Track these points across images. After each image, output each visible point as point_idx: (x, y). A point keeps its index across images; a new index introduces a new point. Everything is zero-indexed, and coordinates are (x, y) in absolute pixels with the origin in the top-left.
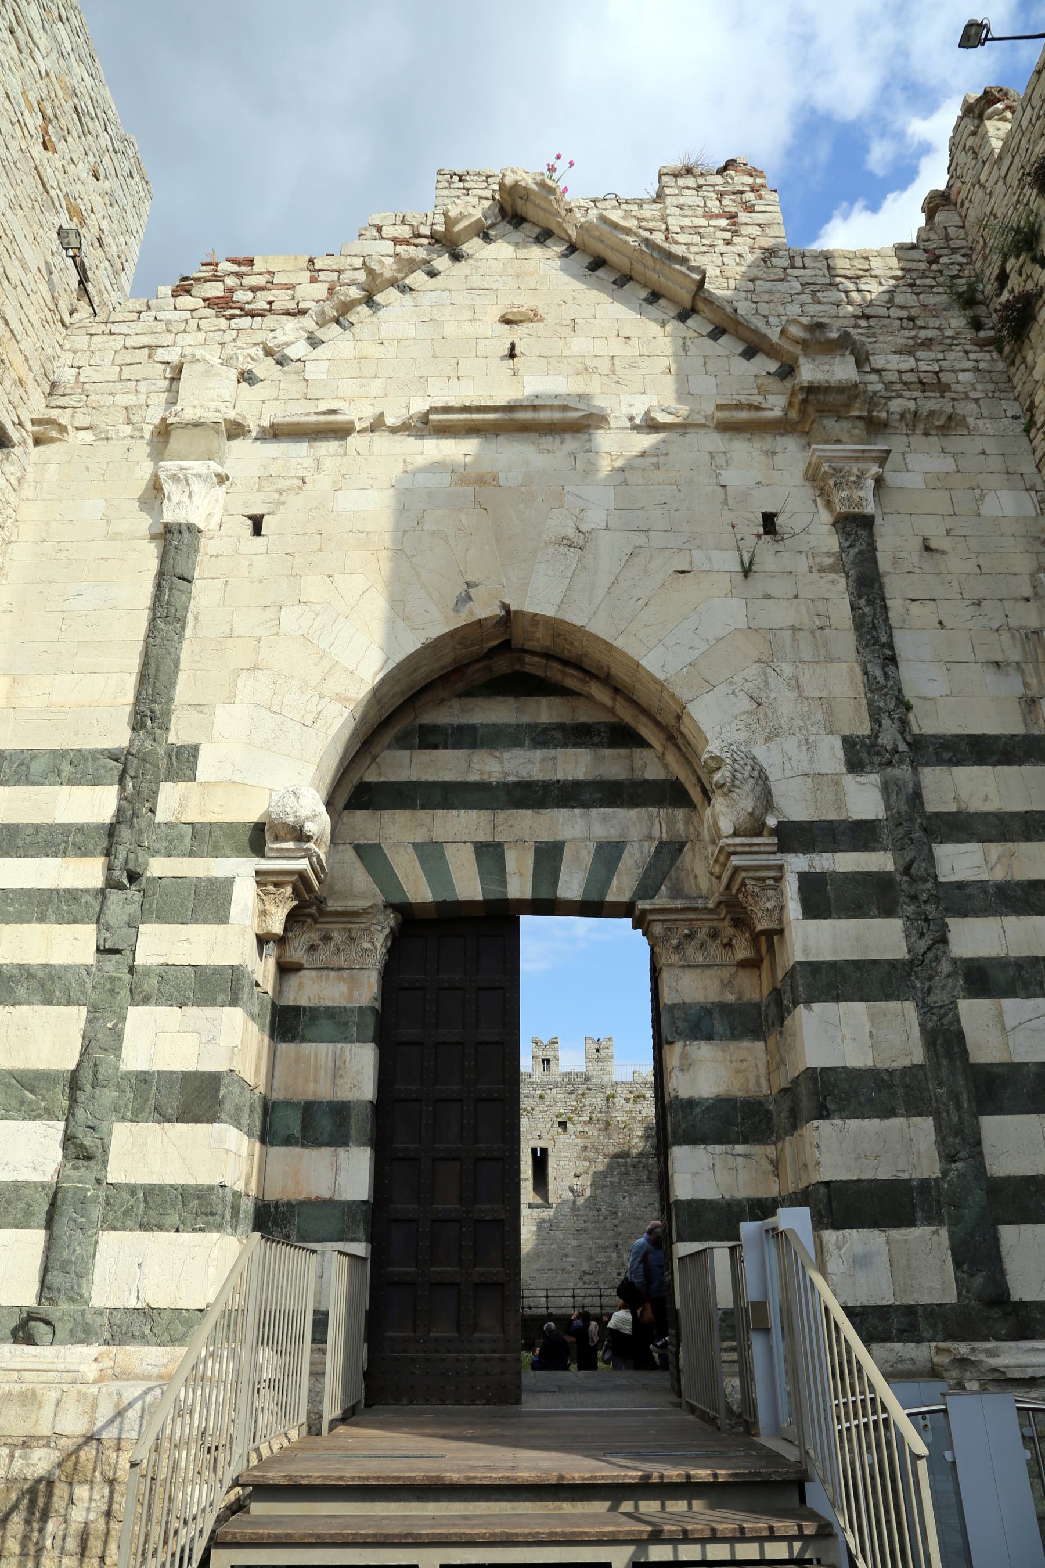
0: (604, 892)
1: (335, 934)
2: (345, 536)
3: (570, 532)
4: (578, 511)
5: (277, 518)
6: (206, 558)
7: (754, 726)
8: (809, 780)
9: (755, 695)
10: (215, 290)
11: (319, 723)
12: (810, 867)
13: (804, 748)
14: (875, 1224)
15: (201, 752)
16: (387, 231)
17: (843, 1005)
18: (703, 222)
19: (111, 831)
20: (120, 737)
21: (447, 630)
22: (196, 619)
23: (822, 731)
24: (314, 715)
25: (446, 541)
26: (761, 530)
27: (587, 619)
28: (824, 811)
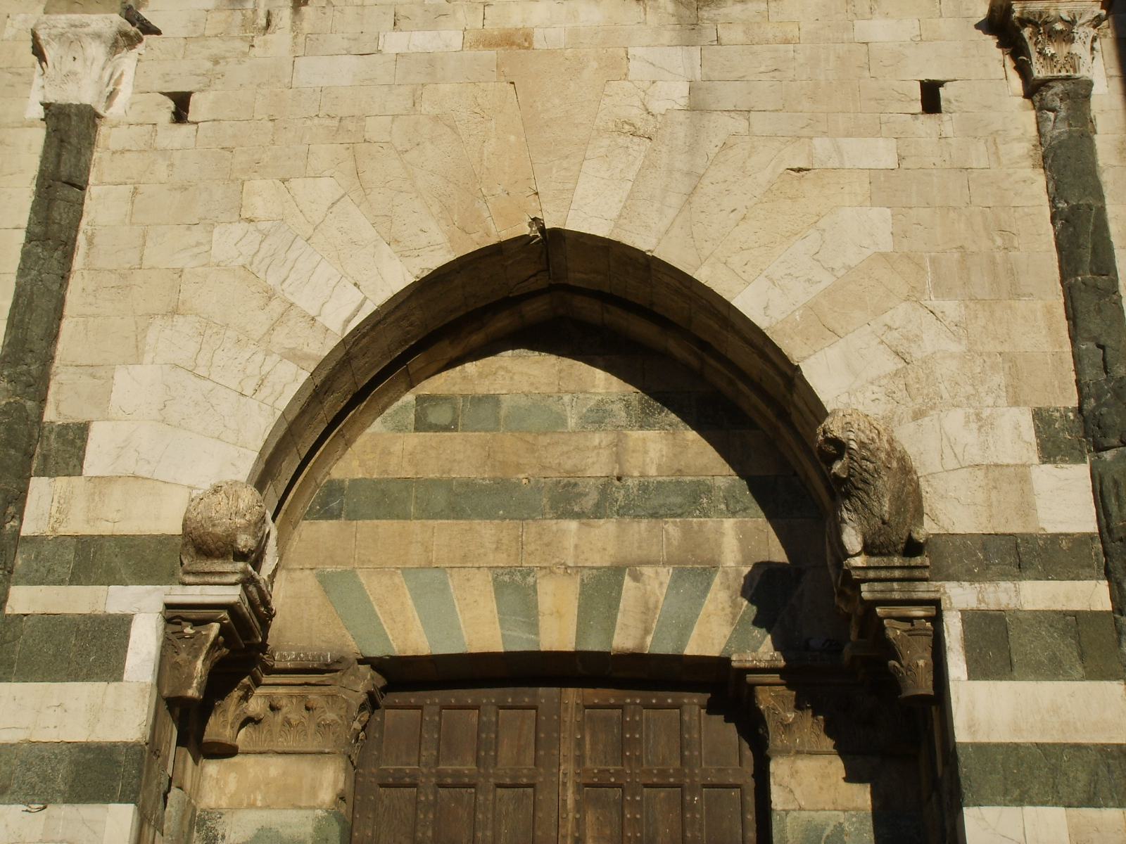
0: (683, 646)
1: (284, 702)
2: (309, 122)
3: (636, 114)
4: (647, 84)
5: (212, 95)
6: (107, 156)
7: (898, 395)
8: (980, 474)
9: (900, 349)
11: (265, 391)
12: (980, 601)
13: (974, 426)
15: (91, 434)
17: (1028, 809)
21: (451, 257)
22: (90, 242)
23: (1002, 401)
24: (256, 380)
25: (454, 129)
26: (918, 107)
27: (654, 241)
28: (1003, 521)
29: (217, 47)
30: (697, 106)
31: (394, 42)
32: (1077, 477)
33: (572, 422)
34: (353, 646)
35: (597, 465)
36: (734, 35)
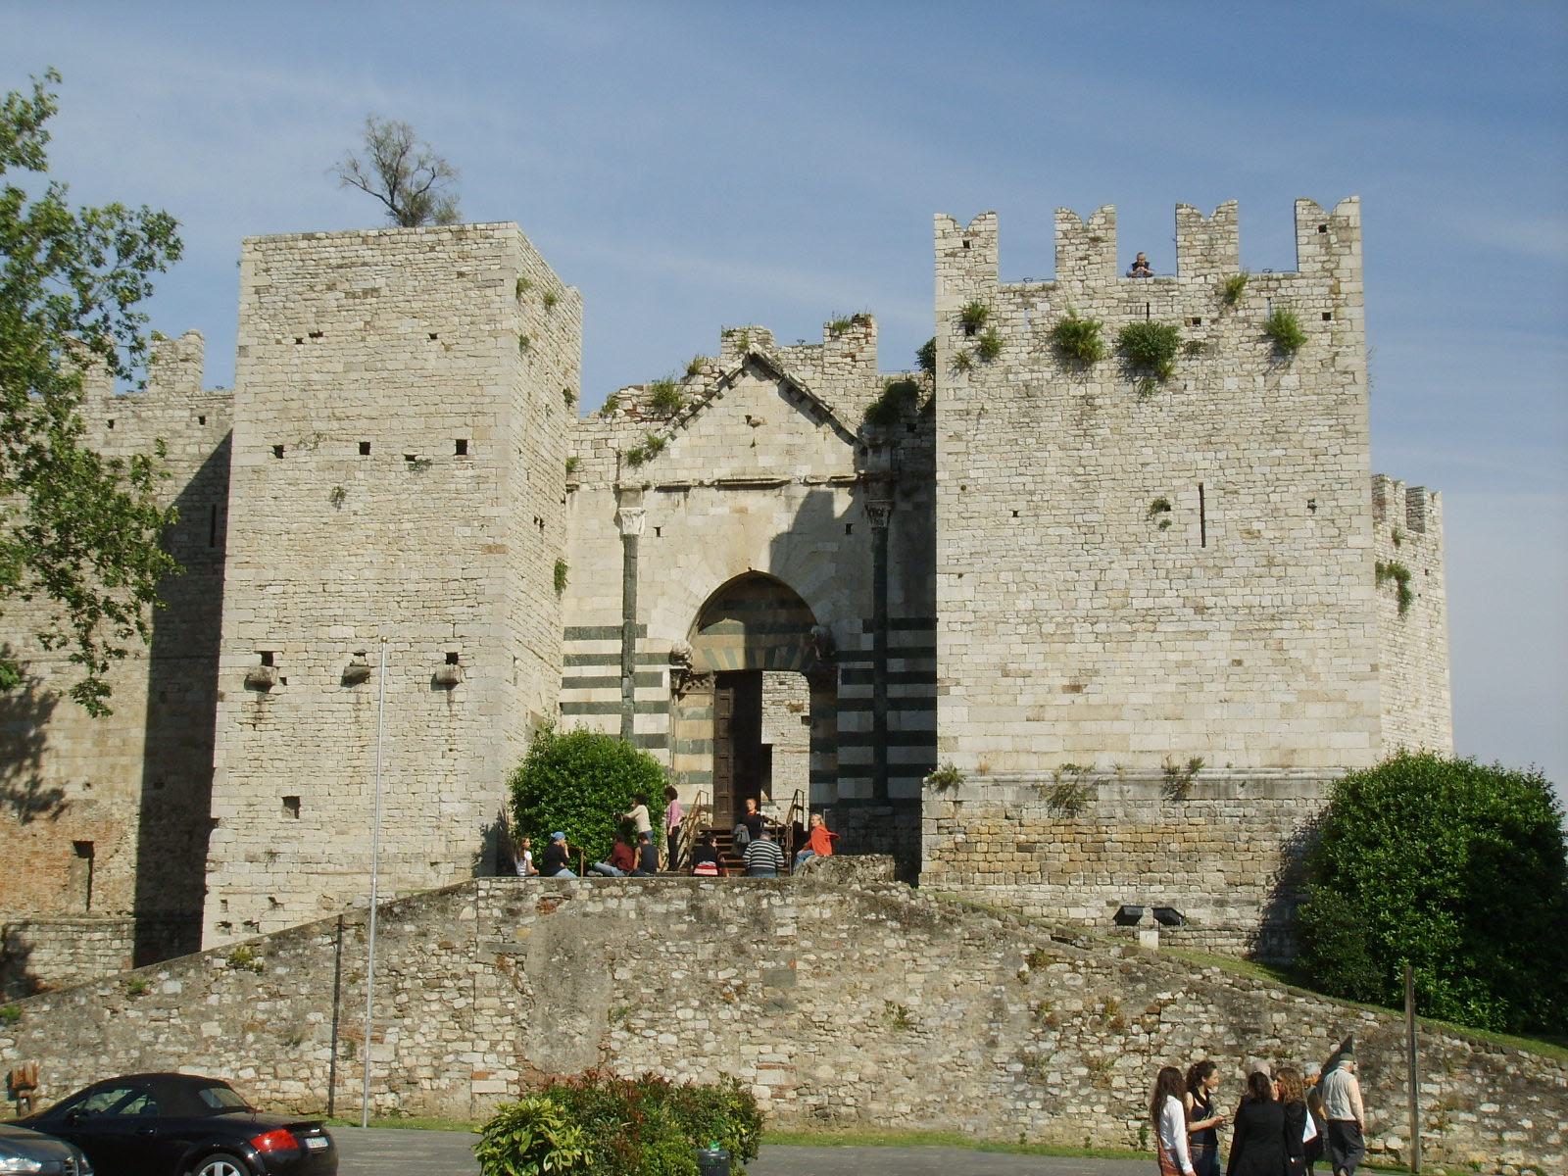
14: (850, 776)
18: (839, 359)
19: (622, 656)
20: (620, 622)
29: (666, 512)
31: (712, 511)
32: (871, 636)
33: (763, 606)
34: (712, 668)
35: (770, 620)
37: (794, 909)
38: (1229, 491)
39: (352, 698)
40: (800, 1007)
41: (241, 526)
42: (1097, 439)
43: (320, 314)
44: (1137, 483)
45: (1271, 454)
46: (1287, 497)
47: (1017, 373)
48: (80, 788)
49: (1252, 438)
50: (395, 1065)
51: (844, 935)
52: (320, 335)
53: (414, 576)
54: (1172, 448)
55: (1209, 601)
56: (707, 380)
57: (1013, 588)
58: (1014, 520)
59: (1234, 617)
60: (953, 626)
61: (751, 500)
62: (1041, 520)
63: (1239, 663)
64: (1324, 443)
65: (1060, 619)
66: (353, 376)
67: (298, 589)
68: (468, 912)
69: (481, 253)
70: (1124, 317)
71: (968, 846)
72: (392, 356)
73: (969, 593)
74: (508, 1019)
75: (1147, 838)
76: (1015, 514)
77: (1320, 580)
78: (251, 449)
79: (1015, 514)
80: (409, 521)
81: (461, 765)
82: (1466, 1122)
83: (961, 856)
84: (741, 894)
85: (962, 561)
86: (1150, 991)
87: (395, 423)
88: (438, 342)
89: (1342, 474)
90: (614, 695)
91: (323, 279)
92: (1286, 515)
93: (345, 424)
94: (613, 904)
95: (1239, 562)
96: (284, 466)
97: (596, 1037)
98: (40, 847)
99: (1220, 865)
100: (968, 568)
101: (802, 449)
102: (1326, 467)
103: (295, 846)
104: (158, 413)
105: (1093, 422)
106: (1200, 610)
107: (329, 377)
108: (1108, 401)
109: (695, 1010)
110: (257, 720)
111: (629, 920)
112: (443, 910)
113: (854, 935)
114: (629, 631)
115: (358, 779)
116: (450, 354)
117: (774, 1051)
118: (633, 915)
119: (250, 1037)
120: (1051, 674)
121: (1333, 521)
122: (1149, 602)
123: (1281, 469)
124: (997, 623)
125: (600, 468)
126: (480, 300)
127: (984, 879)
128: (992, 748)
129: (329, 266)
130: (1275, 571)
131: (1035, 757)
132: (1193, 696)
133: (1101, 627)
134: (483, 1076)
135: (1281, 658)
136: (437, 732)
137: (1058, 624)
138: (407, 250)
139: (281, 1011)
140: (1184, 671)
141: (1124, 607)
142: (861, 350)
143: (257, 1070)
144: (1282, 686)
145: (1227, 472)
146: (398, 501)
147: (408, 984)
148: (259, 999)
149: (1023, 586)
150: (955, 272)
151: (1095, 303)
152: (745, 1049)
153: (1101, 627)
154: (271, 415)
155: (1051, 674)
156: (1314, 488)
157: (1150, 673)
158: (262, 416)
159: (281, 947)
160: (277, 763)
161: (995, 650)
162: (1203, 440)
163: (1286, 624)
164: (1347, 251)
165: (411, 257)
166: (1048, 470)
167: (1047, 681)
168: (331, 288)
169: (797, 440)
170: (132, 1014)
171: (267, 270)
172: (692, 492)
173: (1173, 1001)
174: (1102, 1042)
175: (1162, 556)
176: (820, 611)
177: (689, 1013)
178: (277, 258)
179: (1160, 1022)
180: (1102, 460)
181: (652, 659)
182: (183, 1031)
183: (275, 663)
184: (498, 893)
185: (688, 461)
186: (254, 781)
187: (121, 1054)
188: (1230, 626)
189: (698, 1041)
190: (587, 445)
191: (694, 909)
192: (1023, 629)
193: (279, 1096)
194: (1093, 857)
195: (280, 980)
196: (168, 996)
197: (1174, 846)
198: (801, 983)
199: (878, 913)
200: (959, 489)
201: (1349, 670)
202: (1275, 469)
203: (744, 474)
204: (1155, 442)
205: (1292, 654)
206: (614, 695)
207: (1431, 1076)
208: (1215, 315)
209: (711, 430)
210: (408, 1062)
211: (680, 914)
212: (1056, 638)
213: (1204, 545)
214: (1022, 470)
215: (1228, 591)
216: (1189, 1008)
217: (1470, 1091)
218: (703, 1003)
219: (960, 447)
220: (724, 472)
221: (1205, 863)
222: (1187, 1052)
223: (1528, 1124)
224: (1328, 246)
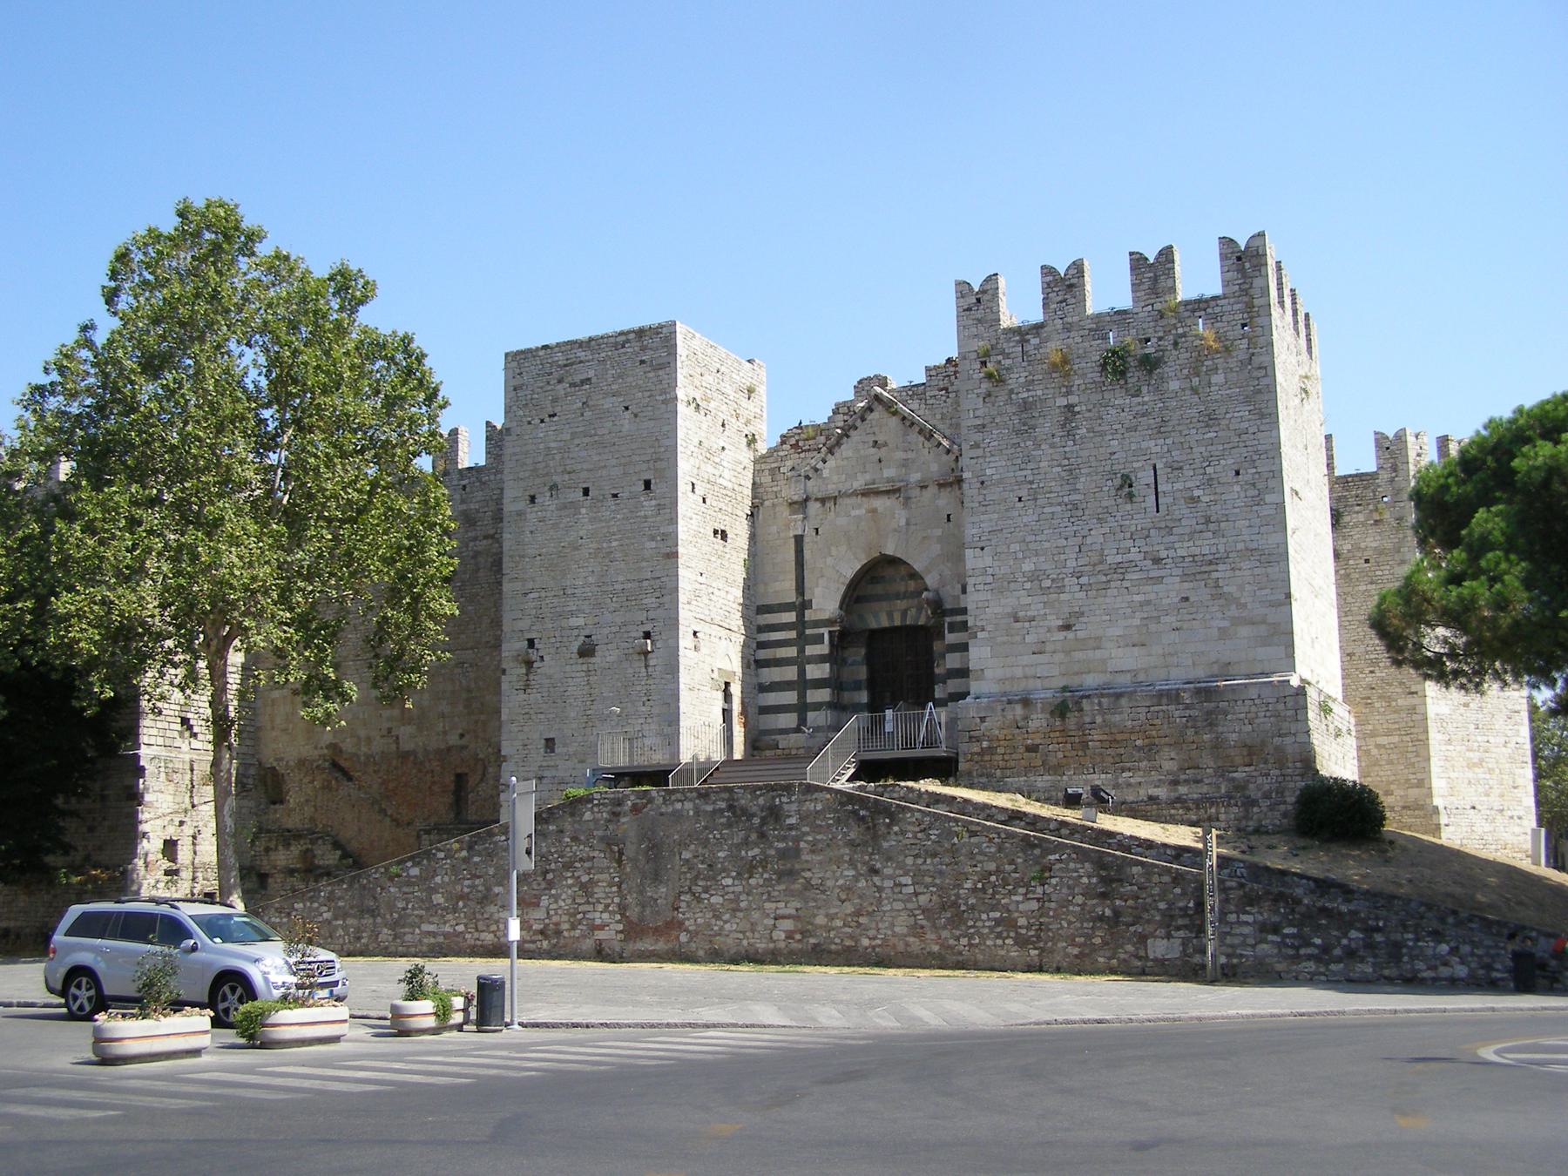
10: (793, 441)
16: (841, 410)
18: (937, 393)
20: (792, 597)
30: (908, 524)
31: (853, 513)
35: (903, 589)
36: (913, 506)
37: (796, 804)
38: (1176, 468)
39: (585, 667)
40: (803, 874)
41: (511, 553)
42: (1077, 437)
43: (555, 400)
44: (1108, 468)
45: (1206, 436)
46: (1219, 469)
47: (1017, 394)
48: (457, 737)
49: (1191, 426)
50: (547, 921)
51: (831, 822)
52: (554, 415)
53: (621, 578)
54: (1132, 440)
55: (1163, 554)
56: (846, 418)
57: (1020, 555)
58: (1021, 504)
59: (1181, 565)
60: (978, 587)
61: (880, 503)
62: (1038, 502)
63: (1187, 599)
64: (1246, 425)
65: (1055, 576)
66: (577, 441)
67: (548, 594)
68: (588, 816)
69: (655, 345)
70: (1093, 343)
71: (991, 750)
72: (600, 425)
73: (988, 561)
74: (615, 889)
75: (1119, 737)
76: (1020, 499)
77: (1245, 531)
78: (515, 499)
79: (1020, 499)
80: (616, 540)
81: (655, 711)
82: (1272, 942)
83: (987, 758)
84: (761, 795)
85: (983, 538)
86: (1043, 856)
87: (604, 472)
88: (630, 412)
89: (1259, 447)
90: (791, 652)
91: (556, 375)
92: (1219, 483)
93: (573, 476)
94: (678, 806)
95: (1184, 522)
96: (536, 509)
97: (671, 899)
98: (435, 779)
99: (1173, 755)
100: (988, 543)
101: (914, 461)
102: (1247, 443)
103: (554, 773)
104: (492, 477)
105: (1074, 425)
106: (1157, 561)
107: (562, 444)
108: (1084, 408)
109: (734, 879)
110: (526, 687)
111: (688, 816)
112: (572, 815)
113: (838, 821)
114: (803, 606)
115: (591, 724)
116: (638, 419)
117: (786, 907)
118: (691, 813)
119: (461, 904)
120: (1049, 617)
121: (1254, 484)
122: (1119, 559)
123: (1213, 448)
124: (1009, 583)
125: (775, 489)
126: (655, 379)
127: (1002, 773)
128: (1008, 675)
129: (559, 366)
130: (1212, 526)
131: (1039, 680)
132: (1153, 627)
133: (1084, 580)
134: (601, 927)
135: (1218, 594)
136: (638, 688)
137: (1053, 580)
138: (607, 349)
139: (477, 886)
140: (1145, 608)
141: (1101, 563)
142: (952, 384)
143: (466, 925)
144: (1219, 615)
145: (1173, 454)
146: (609, 527)
147: (553, 866)
148: (464, 879)
149: (1027, 553)
150: (971, 322)
151: (1072, 334)
152: (767, 905)
153: (1084, 580)
154: (527, 474)
155: (1049, 617)
156: (1238, 460)
157: (1121, 612)
158: (521, 475)
159: (476, 843)
160: (542, 716)
161: (1008, 603)
162: (1155, 431)
163: (1221, 567)
164: (1258, 273)
165: (610, 353)
166: (1042, 464)
167: (1046, 623)
168: (560, 381)
169: (910, 455)
170: (392, 890)
171: (520, 374)
172: (839, 501)
173: (1060, 861)
174: (1010, 893)
175: (1127, 522)
176: (931, 580)
177: (729, 881)
178: (526, 364)
179: (1051, 877)
180: (1081, 453)
181: (817, 624)
182: (422, 901)
183: (536, 646)
184: (606, 801)
185: (835, 478)
186: (526, 729)
187: (388, 916)
188: (1179, 571)
189: (737, 900)
190: (767, 472)
191: (731, 808)
192: (1028, 586)
193: (479, 943)
194: (1080, 753)
195: (476, 864)
196: (413, 877)
197: (1139, 743)
198: (803, 857)
199: (853, 805)
200: (979, 485)
201: (1269, 598)
202: (1209, 448)
203: (874, 484)
204: (1119, 436)
205: (1226, 589)
206: (791, 652)
207: (1248, 908)
208: (1161, 334)
209: (850, 453)
210: (555, 919)
211: (721, 811)
212: (1051, 590)
213: (1158, 511)
214: (1023, 466)
215: (1176, 545)
216: (1072, 865)
217: (1276, 919)
218: (738, 874)
219: (979, 452)
220: (858, 484)
221: (1162, 754)
222: (1070, 898)
223: (1318, 941)
224: (1242, 271)
